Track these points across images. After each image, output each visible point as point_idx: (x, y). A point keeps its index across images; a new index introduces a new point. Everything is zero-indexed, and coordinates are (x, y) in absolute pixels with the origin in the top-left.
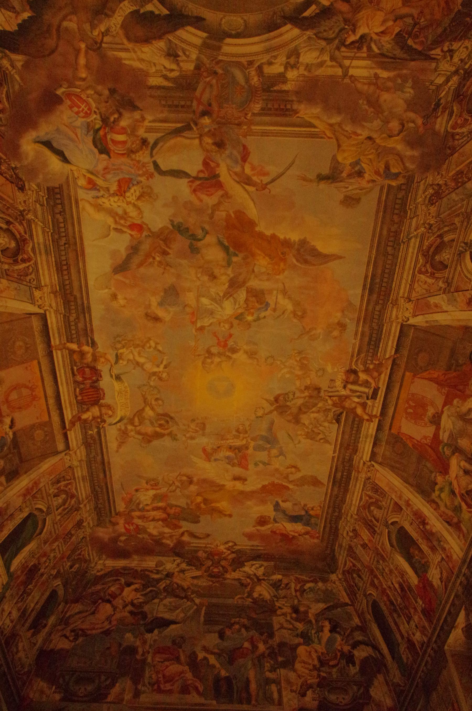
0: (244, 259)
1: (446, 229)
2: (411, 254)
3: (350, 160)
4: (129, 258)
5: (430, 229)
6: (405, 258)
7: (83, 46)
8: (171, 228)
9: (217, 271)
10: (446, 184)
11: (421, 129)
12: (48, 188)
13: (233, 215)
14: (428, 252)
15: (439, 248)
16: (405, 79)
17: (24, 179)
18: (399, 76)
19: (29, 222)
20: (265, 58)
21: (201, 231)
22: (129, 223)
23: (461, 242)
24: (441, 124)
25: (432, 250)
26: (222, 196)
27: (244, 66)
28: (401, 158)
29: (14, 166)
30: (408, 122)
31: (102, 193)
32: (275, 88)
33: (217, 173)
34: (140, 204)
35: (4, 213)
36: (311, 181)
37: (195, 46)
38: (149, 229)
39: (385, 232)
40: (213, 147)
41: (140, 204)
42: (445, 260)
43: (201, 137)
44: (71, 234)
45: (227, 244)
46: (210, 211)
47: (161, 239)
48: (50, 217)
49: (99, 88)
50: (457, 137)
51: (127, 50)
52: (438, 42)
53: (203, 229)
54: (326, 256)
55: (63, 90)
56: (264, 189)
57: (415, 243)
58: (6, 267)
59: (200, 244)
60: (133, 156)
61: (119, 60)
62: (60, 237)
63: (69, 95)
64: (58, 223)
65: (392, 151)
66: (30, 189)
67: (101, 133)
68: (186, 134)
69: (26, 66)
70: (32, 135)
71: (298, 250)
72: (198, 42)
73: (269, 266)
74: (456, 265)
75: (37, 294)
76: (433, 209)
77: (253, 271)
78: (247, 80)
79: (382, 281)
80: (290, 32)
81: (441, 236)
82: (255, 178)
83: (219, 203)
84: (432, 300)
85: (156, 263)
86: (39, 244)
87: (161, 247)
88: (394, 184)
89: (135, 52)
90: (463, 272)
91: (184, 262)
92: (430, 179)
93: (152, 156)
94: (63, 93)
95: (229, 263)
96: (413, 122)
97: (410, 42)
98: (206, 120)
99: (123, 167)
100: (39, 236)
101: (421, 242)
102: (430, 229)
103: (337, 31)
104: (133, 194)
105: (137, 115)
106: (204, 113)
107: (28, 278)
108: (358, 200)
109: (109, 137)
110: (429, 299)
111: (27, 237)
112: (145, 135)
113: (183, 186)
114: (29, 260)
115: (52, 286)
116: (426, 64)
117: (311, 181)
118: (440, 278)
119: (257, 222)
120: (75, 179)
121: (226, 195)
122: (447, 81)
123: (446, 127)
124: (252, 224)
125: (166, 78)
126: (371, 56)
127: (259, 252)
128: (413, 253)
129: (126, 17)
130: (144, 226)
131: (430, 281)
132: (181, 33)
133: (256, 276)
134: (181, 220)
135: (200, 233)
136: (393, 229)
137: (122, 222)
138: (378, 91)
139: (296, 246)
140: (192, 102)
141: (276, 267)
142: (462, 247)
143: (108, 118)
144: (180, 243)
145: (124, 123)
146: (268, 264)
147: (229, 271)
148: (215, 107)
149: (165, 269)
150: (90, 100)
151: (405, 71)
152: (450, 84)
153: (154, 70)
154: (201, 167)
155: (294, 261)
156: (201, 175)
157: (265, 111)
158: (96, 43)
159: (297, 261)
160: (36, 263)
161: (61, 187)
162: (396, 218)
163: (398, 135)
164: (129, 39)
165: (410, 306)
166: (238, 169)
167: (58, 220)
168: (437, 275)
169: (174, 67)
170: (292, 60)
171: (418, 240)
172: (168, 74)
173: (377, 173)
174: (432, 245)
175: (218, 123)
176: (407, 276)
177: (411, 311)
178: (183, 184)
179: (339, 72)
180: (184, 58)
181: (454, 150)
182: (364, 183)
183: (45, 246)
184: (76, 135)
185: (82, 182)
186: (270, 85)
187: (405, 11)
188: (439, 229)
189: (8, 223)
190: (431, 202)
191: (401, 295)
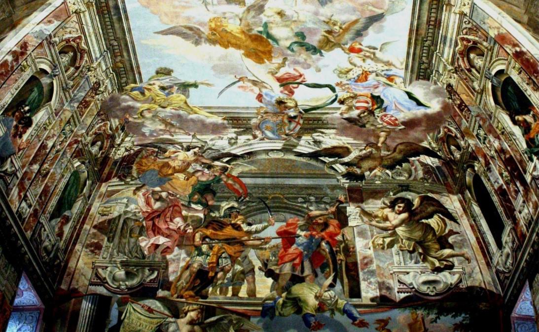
0: (251, 29)
1: (76, 74)
2: (95, 46)
3: (175, 95)
4: (366, 28)
5: (89, 68)
6: (97, 40)
7: (379, 145)
8: (322, 51)
9: (278, 18)
10: (93, 97)
11: (128, 116)
12: (428, 80)
13: (266, 60)
14: (81, 54)
15: (73, 61)
16: (151, 135)
17: (446, 91)
18: (155, 136)
19: (452, 63)
20: (252, 141)
21: (294, 49)
22: (363, 53)
23: (59, 74)
24: (115, 123)
25: (79, 57)
26: (277, 73)
27: (267, 138)
28: (135, 99)
29: (450, 100)
30: (139, 117)
31: (383, 73)
32: (242, 129)
33: (282, 88)
34: (351, 67)
35: (470, 79)
36: (202, 84)
37: (301, 146)
38: (343, 50)
39: (125, 54)
40: (286, 101)
41: (351, 67)
42: (64, 56)
43: (296, 106)
44: (419, 48)
45: (270, 40)
46: (287, 63)
47: (332, 42)
48: (434, 62)
49: (372, 128)
50: (100, 121)
51: (348, 143)
52: (139, 152)
53: (292, 50)
54: (172, 34)
55: (400, 128)
56: (240, 78)
57: (94, 52)
58: (485, 43)
59: (295, 39)
60: (352, 95)
61: (355, 139)
62: (429, 46)
63: (396, 125)
64: (427, 58)
65: (145, 102)
66: (444, 83)
67: (376, 107)
68: (308, 107)
69: (422, 141)
70: (429, 111)
71: (200, 37)
72: (299, 147)
73: (226, 25)
74: (53, 59)
75: (466, 10)
76: (94, 80)
77: (241, 20)
78: (263, 132)
79: (111, 18)
80: (238, 151)
81: (77, 68)
82: (250, 84)
83: (279, 68)
84: (56, 23)
85: (339, 24)
86: (450, 46)
87: (333, 36)
88: (133, 85)
89: (344, 143)
90: (45, 59)
91: (310, 25)
92: (106, 95)
93: (337, 96)
94: (400, 126)
95: (266, 25)
96: (135, 118)
97: (157, 150)
98: (292, 114)
99: (362, 89)
100: (448, 53)
101: (90, 56)
102: (89, 68)
103: (206, 153)
104: (357, 72)
105: (346, 116)
106: (295, 117)
107: (469, 26)
108: (157, 73)
109: (370, 105)
110: (60, 23)
111: (458, 55)
112: (341, 106)
113: (311, 76)
114: (463, 39)
115: (450, 11)
116: (140, 143)
117: (202, 84)
118: (60, 43)
119: (243, 56)
120: (404, 82)
121: (273, 74)
122: (123, 140)
123: (111, 122)
124: (248, 55)
125: (323, 133)
126: (180, 144)
127: (237, 35)
128: (93, 47)
129: (348, 156)
130: (347, 51)
131: (67, 36)
132: (311, 151)
133: (237, 16)
134: (313, 57)
135: (295, 47)
136: (119, 58)
137: (368, 54)
138: (168, 129)
139: (203, 40)
140: (303, 122)
141: (219, 24)
142: (57, 72)
143: (368, 114)
144: (314, 40)
145: (357, 112)
146: (227, 26)
147: (265, 19)
148: (286, 121)
149: (330, 20)
150: (380, 122)
151: (153, 138)
152: (120, 139)
153: (331, 136)
154: (295, 90)
155: (202, 29)
156: (295, 85)
157: (249, 119)
158: (370, 146)
159: (199, 29)
160: (458, 34)
161: (418, 78)
162: (120, 65)
163: (143, 111)
164: (347, 148)
165: (73, 8)
166: (264, 91)
167: (427, 59)
168: (64, 43)
169: (316, 138)
170: (233, 141)
171: (94, 57)
172: (321, 134)
173: (149, 90)
174: (80, 59)
175: (284, 113)
176: (89, 29)
177: (69, 5)
178: (309, 81)
179: (198, 137)
180: (309, 141)
181: (98, 114)
182: (158, 83)
183: (445, 43)
184: (396, 105)
185: (399, 80)
186: (247, 130)
187: (166, 160)
188: (82, 71)
189: (469, 71)
190: (98, 84)
191: (87, 13)
